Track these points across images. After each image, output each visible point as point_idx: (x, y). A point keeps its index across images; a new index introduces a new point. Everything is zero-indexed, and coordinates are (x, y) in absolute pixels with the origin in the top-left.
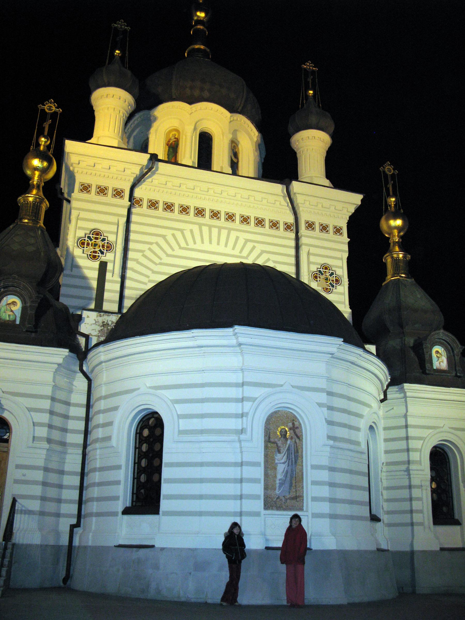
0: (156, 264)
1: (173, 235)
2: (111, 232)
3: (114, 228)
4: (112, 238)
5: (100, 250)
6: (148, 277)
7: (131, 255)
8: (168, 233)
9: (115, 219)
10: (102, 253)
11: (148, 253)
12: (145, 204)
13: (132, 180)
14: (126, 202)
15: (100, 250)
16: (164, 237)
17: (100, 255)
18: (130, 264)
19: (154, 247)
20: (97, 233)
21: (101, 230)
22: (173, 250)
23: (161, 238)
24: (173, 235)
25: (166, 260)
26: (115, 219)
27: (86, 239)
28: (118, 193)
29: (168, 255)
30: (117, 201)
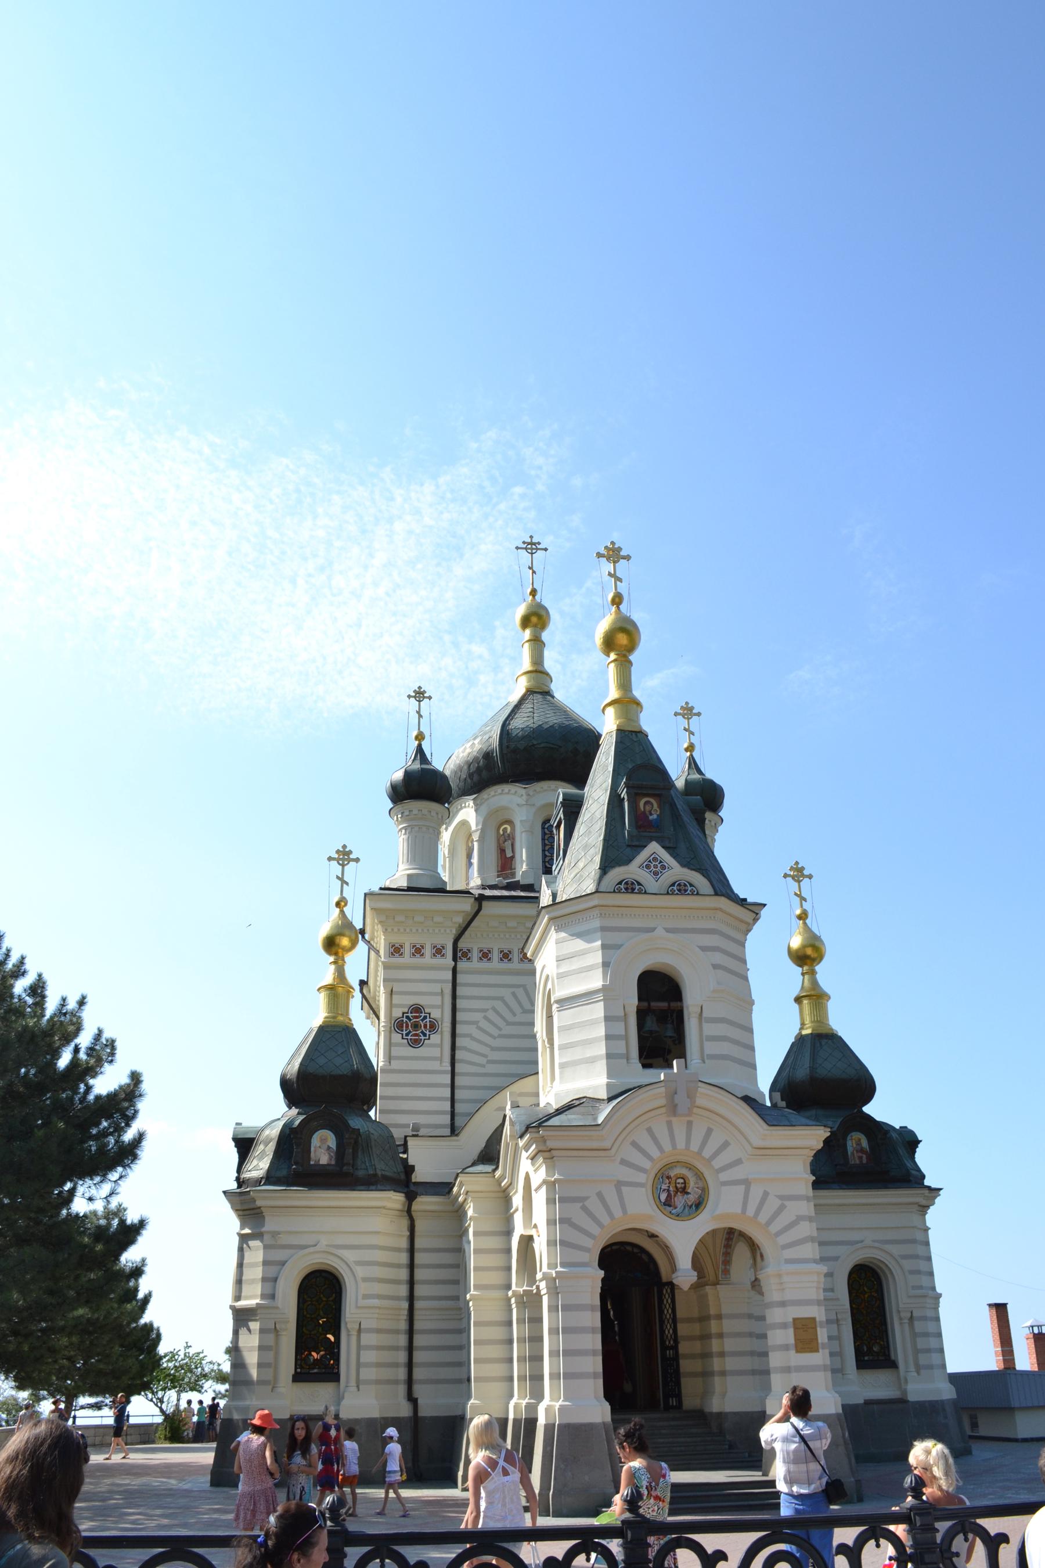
0: (494, 1038)
1: (514, 994)
2: (434, 1007)
3: (437, 1000)
4: (436, 1014)
5: (422, 1032)
6: (485, 1056)
7: (459, 1029)
8: (506, 993)
9: (436, 988)
10: (425, 1035)
11: (484, 1024)
12: (475, 955)
13: (454, 932)
14: (449, 961)
15: (422, 1032)
16: (502, 999)
17: (423, 1038)
18: (459, 1042)
19: (491, 1014)
20: (417, 1009)
21: (421, 1003)
22: (514, 1015)
23: (500, 1002)
24: (514, 994)
25: (508, 1030)
26: (436, 988)
27: (405, 1019)
28: (439, 951)
29: (508, 1023)
30: (438, 961)
